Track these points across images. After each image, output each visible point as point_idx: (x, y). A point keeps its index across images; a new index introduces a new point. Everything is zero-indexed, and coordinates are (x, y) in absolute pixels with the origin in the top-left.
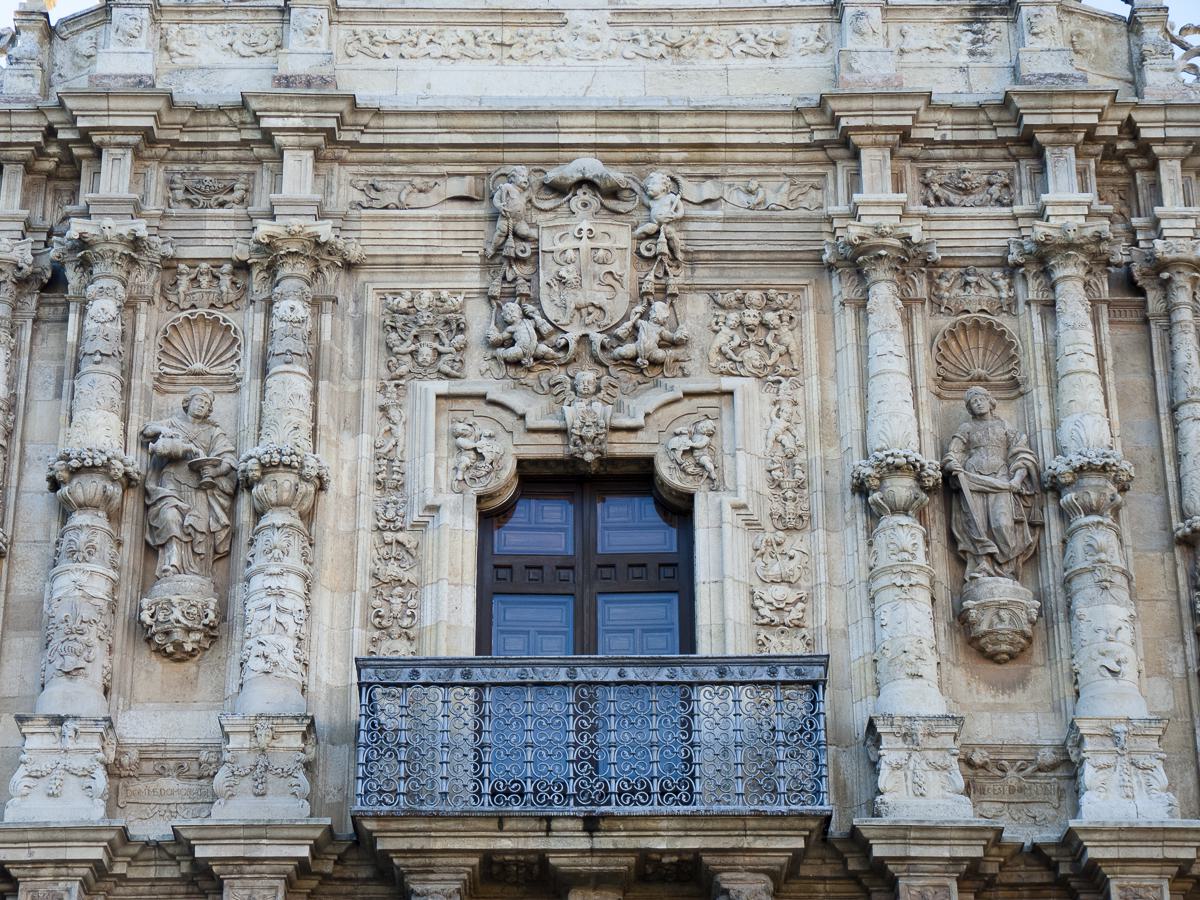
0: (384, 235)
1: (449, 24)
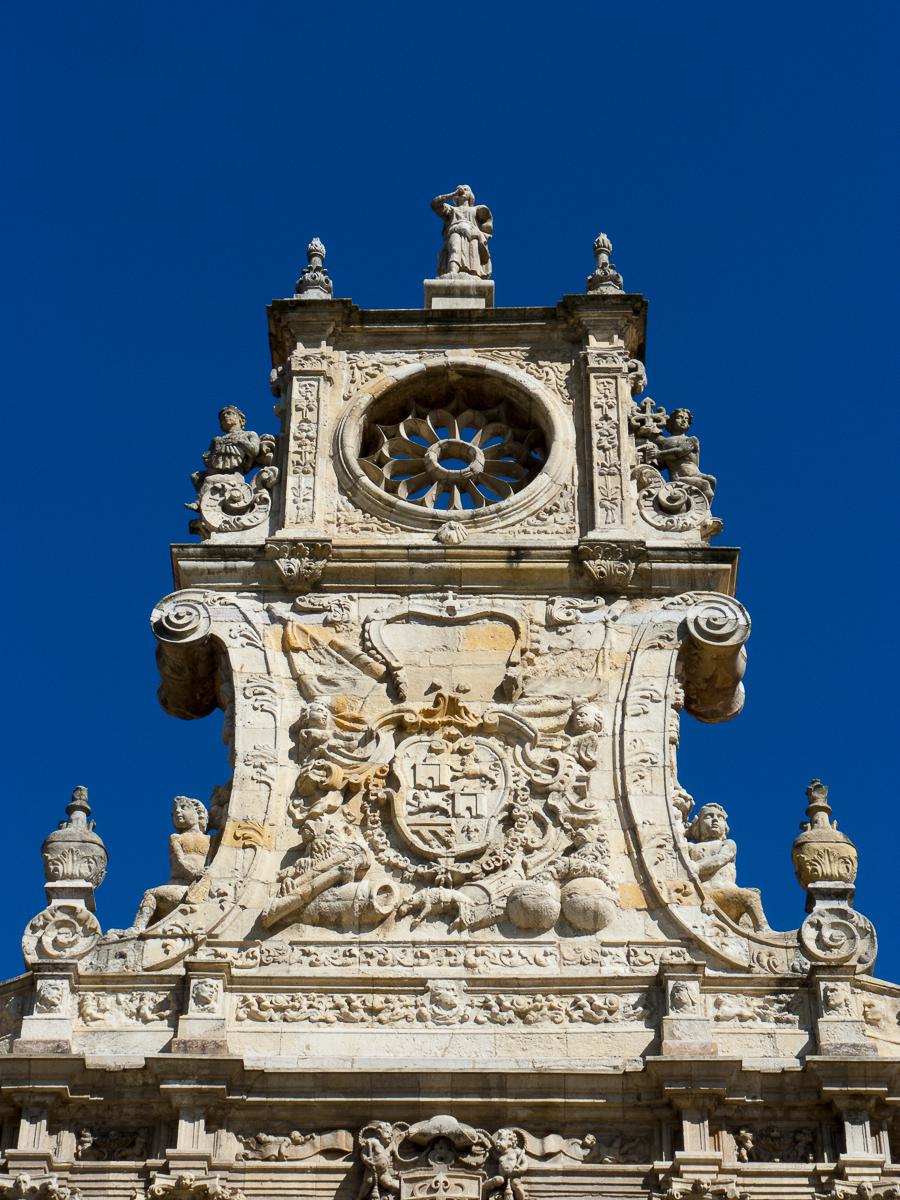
0: (265, 1185)
1: (326, 992)
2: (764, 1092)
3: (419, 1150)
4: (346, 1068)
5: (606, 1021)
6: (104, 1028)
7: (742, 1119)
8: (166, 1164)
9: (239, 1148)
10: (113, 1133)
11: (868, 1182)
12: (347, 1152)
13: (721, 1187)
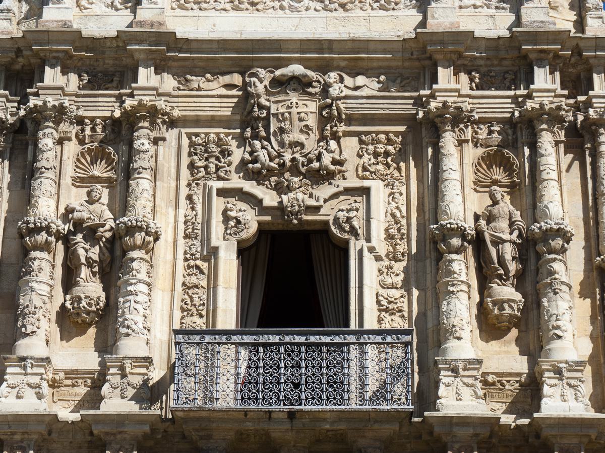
2: (487, 49)
3: (281, 85)
4: (237, 37)
5: (394, 9)
6: (92, 14)
7: (473, 66)
8: (132, 92)
9: (175, 83)
10: (100, 74)
11: (546, 101)
12: (238, 86)
13: (459, 104)
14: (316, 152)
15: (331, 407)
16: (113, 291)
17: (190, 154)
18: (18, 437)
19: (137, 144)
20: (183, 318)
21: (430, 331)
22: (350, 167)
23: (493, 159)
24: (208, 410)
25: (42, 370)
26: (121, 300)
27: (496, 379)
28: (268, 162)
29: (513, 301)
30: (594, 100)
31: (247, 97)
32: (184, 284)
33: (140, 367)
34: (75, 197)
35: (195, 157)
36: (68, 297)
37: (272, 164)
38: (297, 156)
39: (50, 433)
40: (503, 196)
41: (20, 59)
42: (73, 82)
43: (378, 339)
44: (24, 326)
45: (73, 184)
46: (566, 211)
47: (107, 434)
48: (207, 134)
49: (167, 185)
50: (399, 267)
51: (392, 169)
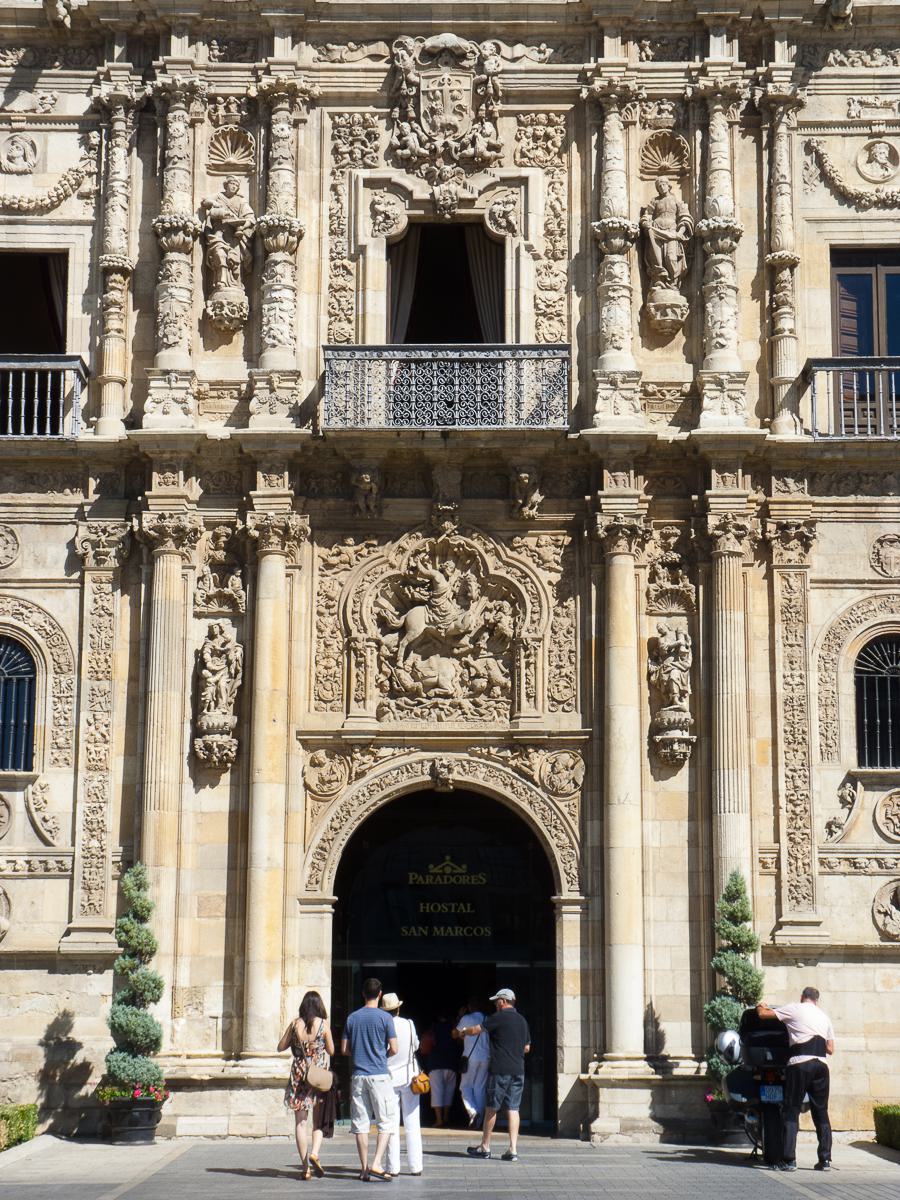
3: (432, 57)
14: (471, 136)
15: (485, 426)
16: (256, 295)
17: (333, 138)
18: (167, 456)
19: (276, 129)
20: (330, 323)
21: (589, 337)
22: (506, 152)
23: (666, 144)
24: (361, 431)
25: (186, 384)
26: (266, 307)
27: (656, 388)
28: (418, 147)
29: (678, 306)
30: (774, 73)
31: (395, 74)
32: (331, 286)
33: (288, 380)
34: (211, 189)
35: (339, 141)
36: (209, 303)
37: (422, 151)
38: (450, 140)
39: (199, 451)
40: (670, 187)
41: (142, 24)
42: (202, 53)
43: (535, 354)
44: (165, 336)
45: (208, 173)
46: (737, 202)
47: (258, 452)
48: (351, 114)
49: (309, 174)
50: (562, 266)
51: (552, 154)
